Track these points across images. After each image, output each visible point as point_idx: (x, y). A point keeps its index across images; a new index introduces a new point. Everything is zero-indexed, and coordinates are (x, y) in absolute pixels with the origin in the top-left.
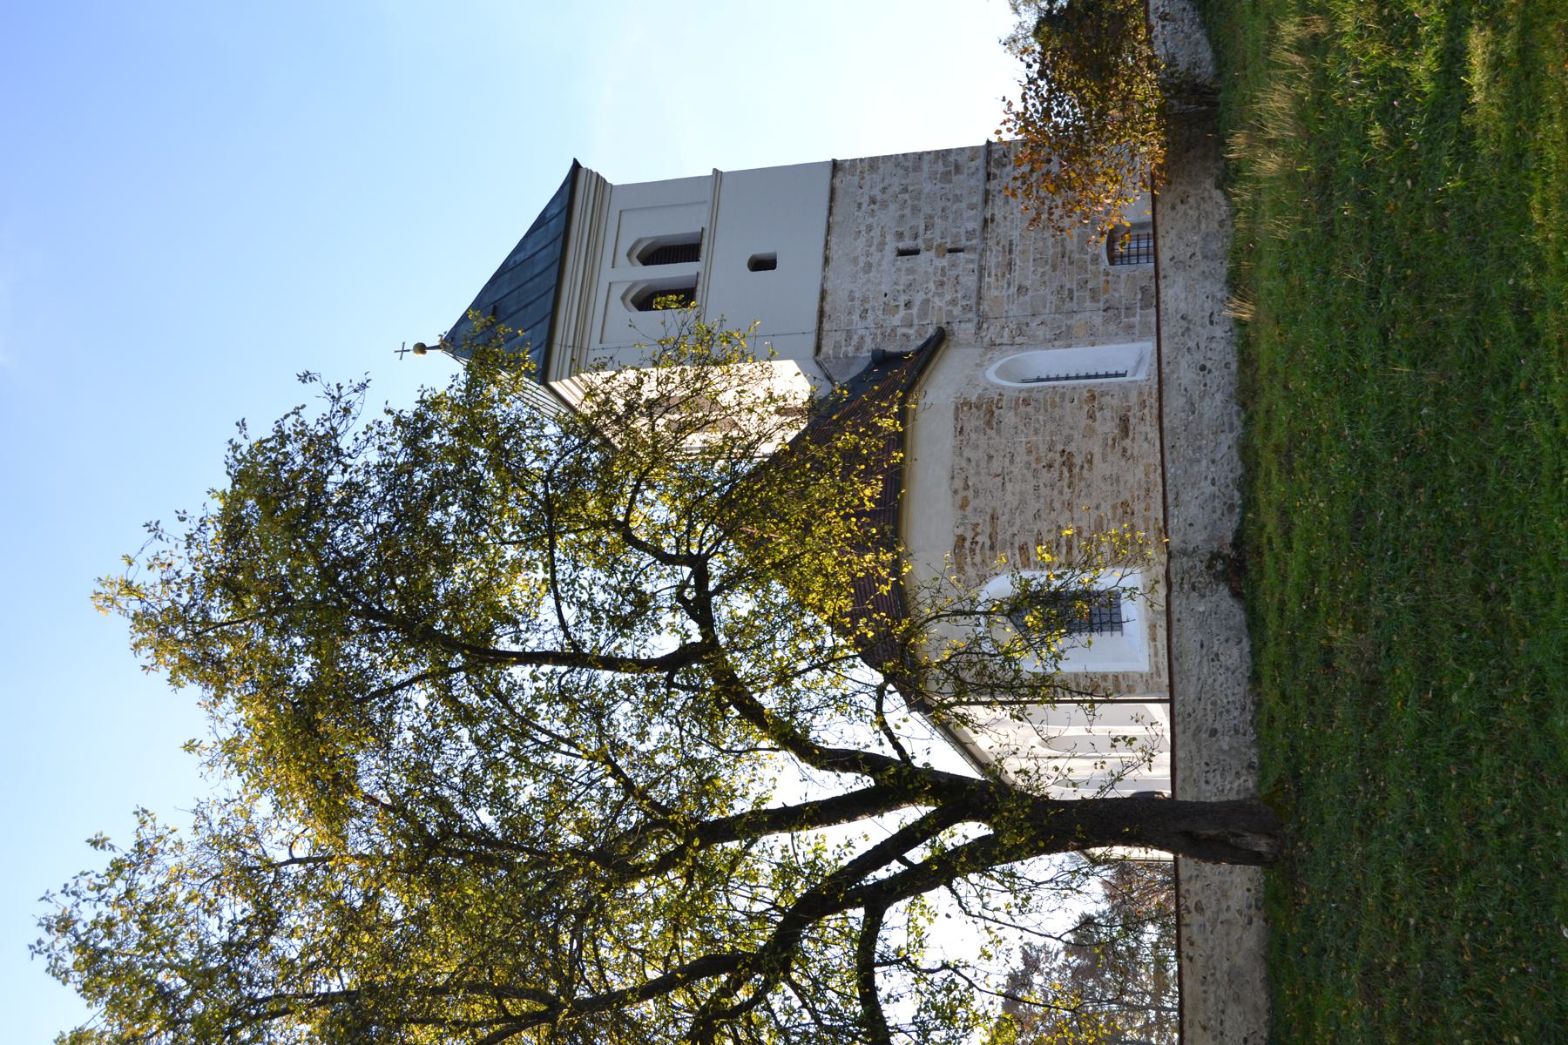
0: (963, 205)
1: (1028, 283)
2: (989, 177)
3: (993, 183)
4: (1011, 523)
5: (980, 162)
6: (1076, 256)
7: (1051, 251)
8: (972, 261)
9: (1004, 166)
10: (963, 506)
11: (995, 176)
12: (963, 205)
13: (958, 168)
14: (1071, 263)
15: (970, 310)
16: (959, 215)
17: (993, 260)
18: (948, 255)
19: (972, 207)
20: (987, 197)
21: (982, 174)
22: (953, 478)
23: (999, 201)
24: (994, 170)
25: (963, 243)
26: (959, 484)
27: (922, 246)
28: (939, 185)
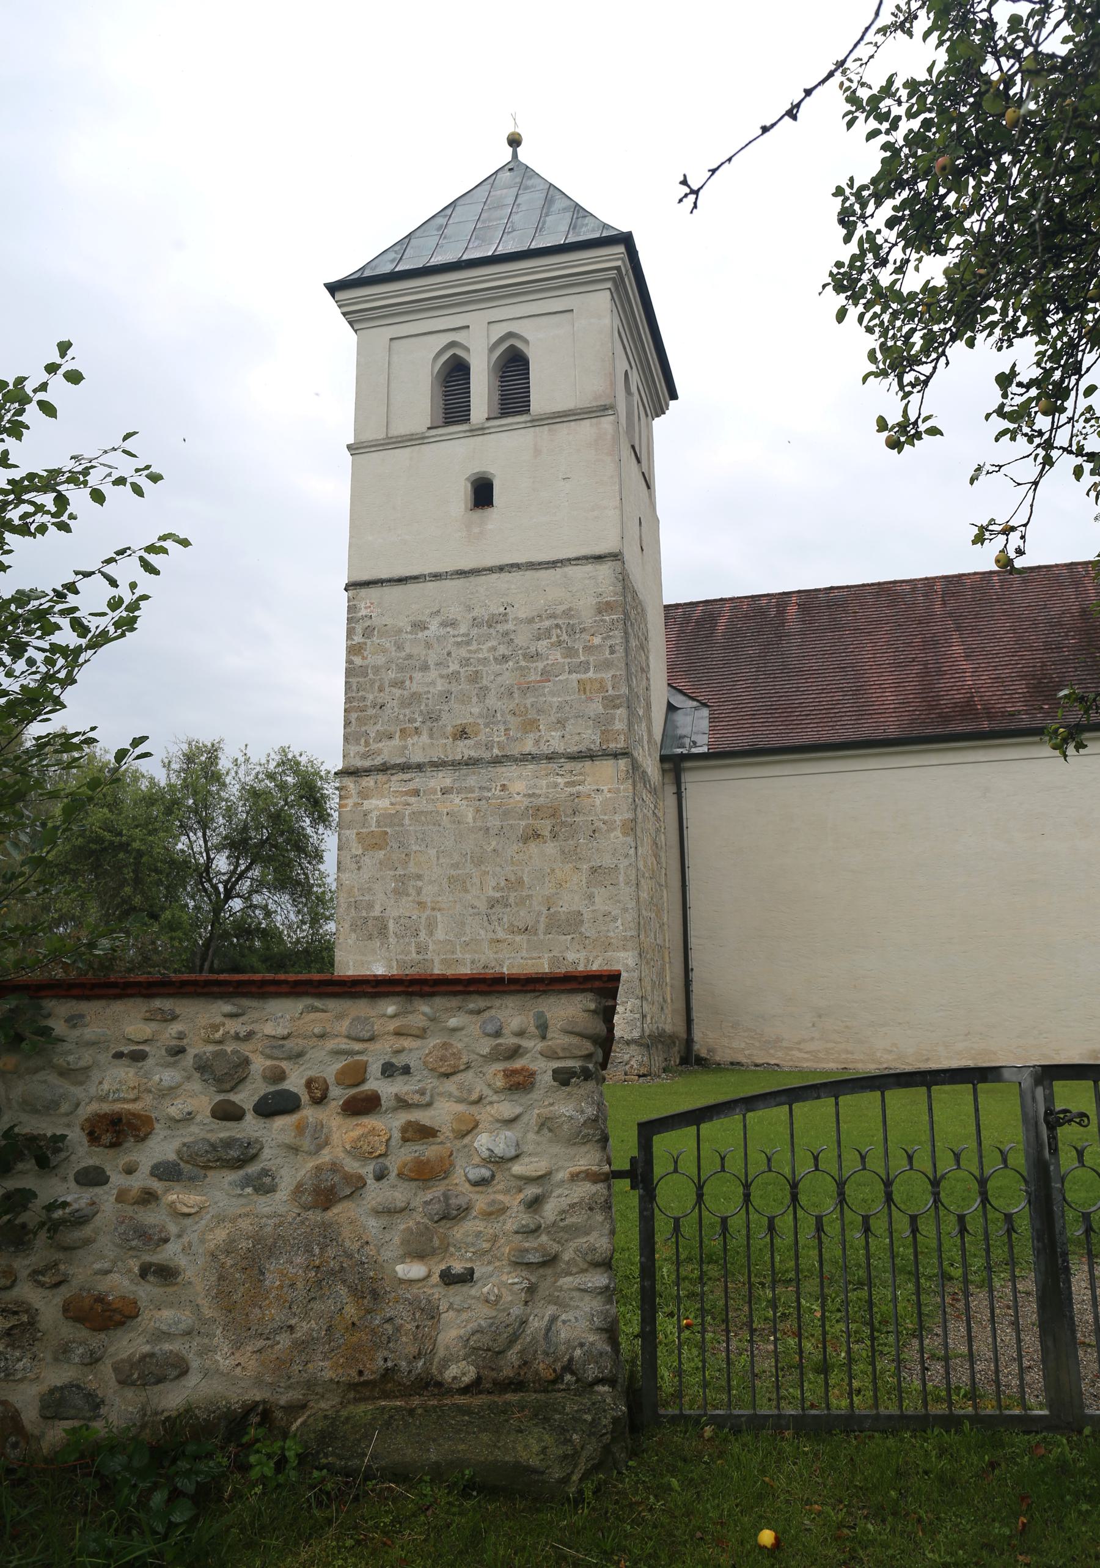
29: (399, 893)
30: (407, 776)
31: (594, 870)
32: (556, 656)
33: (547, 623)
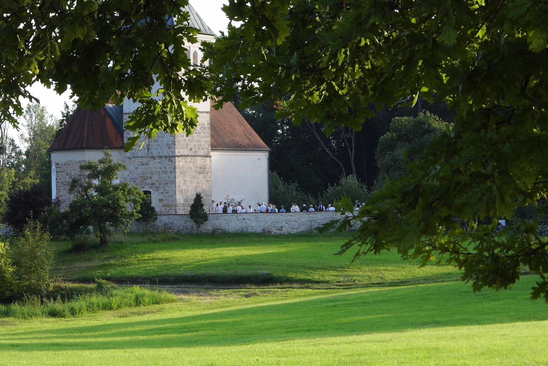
0: (160, 150)
1: (138, 170)
2: (166, 157)
3: (164, 158)
4: (61, 176)
5: (171, 154)
6: (144, 182)
7: (146, 176)
8: (145, 154)
9: (169, 161)
10: (65, 164)
11: (166, 159)
12: (160, 150)
13: (169, 148)
14: (142, 181)
15: (133, 155)
16: (157, 149)
17: (145, 160)
18: (147, 147)
19: (159, 153)
20: (160, 157)
21: (167, 155)
22: (70, 161)
23: (160, 161)
24: (168, 158)
25: (150, 151)
26: (69, 163)
27: (150, 140)
28: (165, 143)
29: (184, 184)
30: (184, 158)
31: (207, 180)
32: (202, 134)
33: (201, 126)
